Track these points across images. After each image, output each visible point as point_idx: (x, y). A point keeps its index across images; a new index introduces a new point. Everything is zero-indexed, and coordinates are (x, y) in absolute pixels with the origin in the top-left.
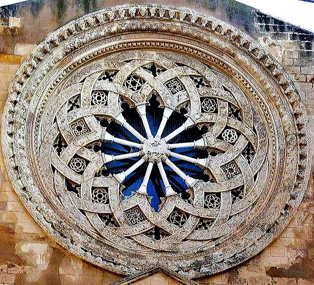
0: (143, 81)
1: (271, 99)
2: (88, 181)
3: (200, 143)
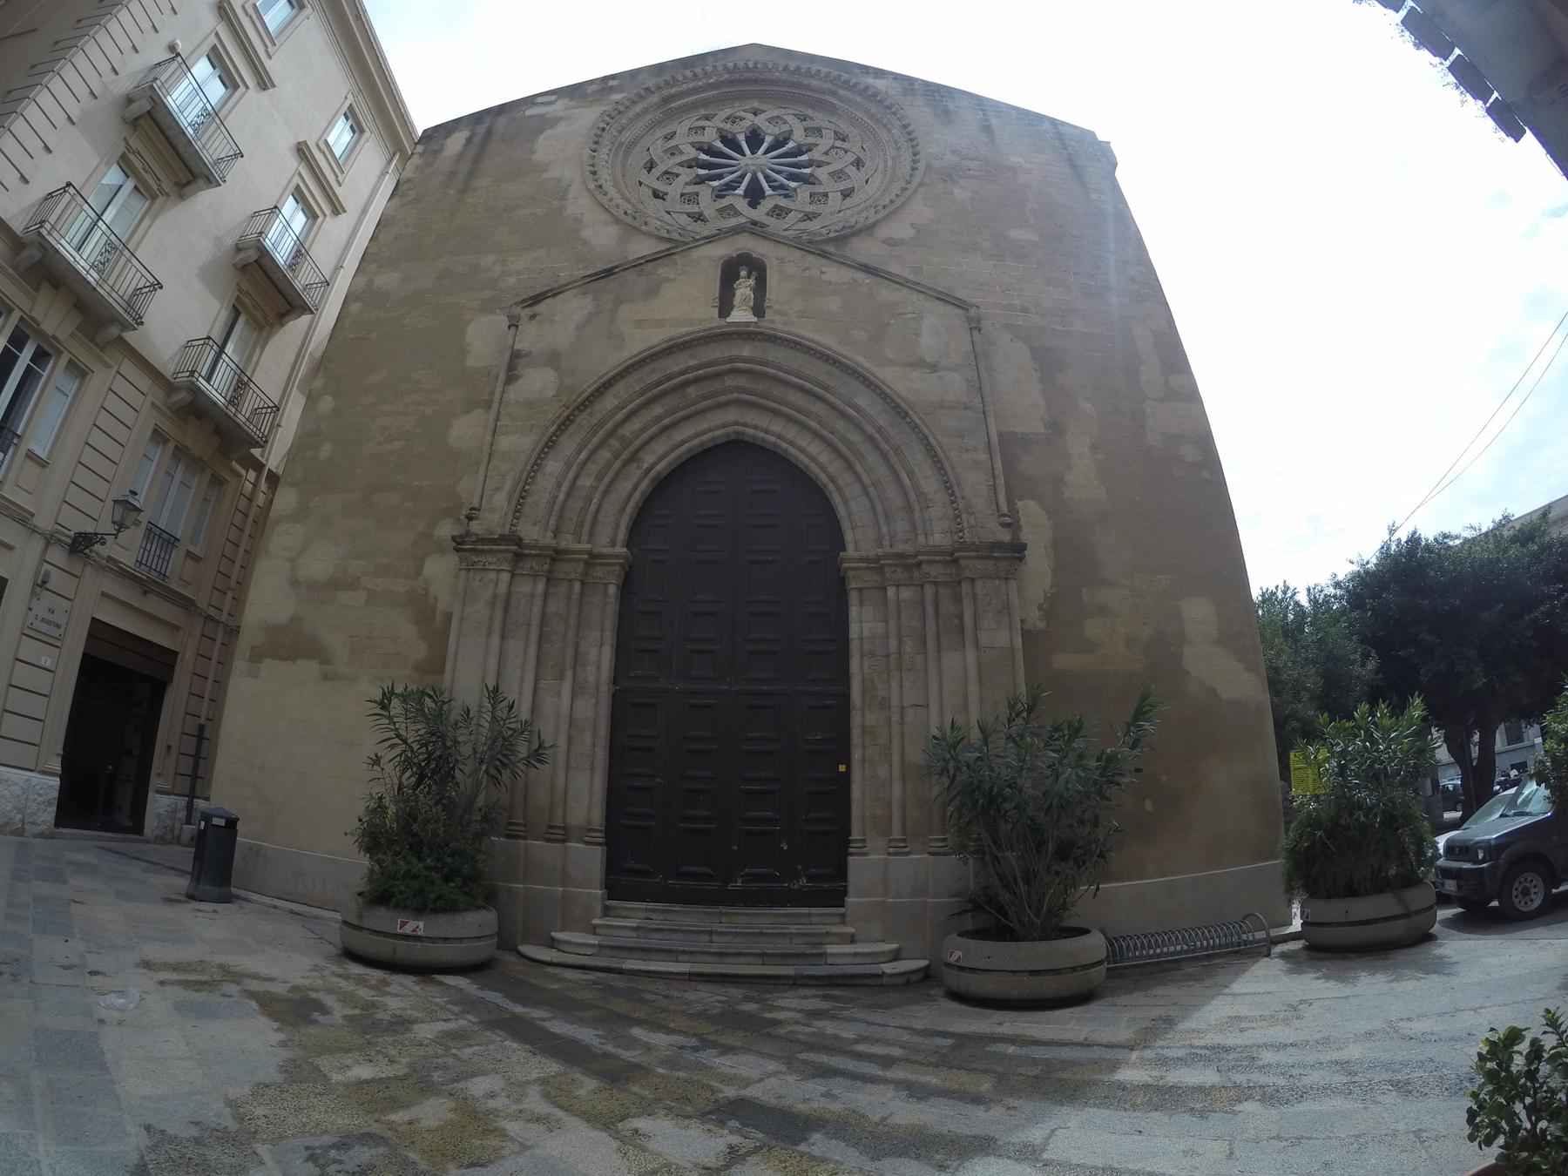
0: (742, 119)
1: (878, 121)
3: (804, 158)
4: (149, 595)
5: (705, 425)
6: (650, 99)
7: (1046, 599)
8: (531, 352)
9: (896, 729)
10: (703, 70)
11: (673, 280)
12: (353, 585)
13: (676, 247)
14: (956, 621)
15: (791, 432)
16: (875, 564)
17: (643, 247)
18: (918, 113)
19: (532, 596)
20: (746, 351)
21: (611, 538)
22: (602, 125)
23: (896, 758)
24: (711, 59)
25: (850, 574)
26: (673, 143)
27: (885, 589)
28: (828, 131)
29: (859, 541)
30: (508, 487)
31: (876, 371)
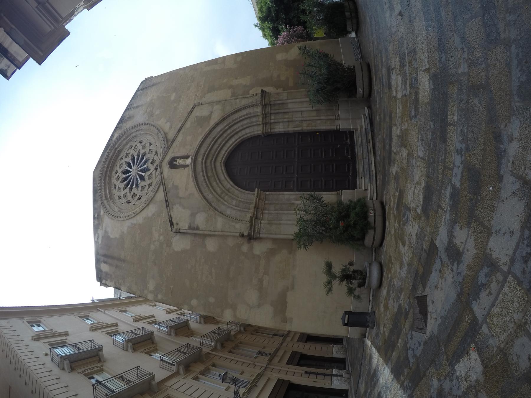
1: (128, 136)
2: (138, 192)
3: (136, 157)
4: (257, 385)
5: (220, 171)
6: (105, 203)
7: (275, 88)
8: (189, 223)
9: (308, 118)
10: (99, 187)
11: (173, 182)
12: (261, 281)
13: (162, 182)
14: (280, 105)
15: (225, 148)
16: (265, 124)
17: (160, 195)
18: (128, 125)
19: (269, 213)
20: (200, 159)
21: (252, 196)
22: (112, 216)
23: (315, 118)
24: (96, 185)
25: (266, 131)
26: (122, 197)
27: (271, 123)
28: (128, 151)
29: (258, 130)
30: (234, 224)
31: (211, 126)
